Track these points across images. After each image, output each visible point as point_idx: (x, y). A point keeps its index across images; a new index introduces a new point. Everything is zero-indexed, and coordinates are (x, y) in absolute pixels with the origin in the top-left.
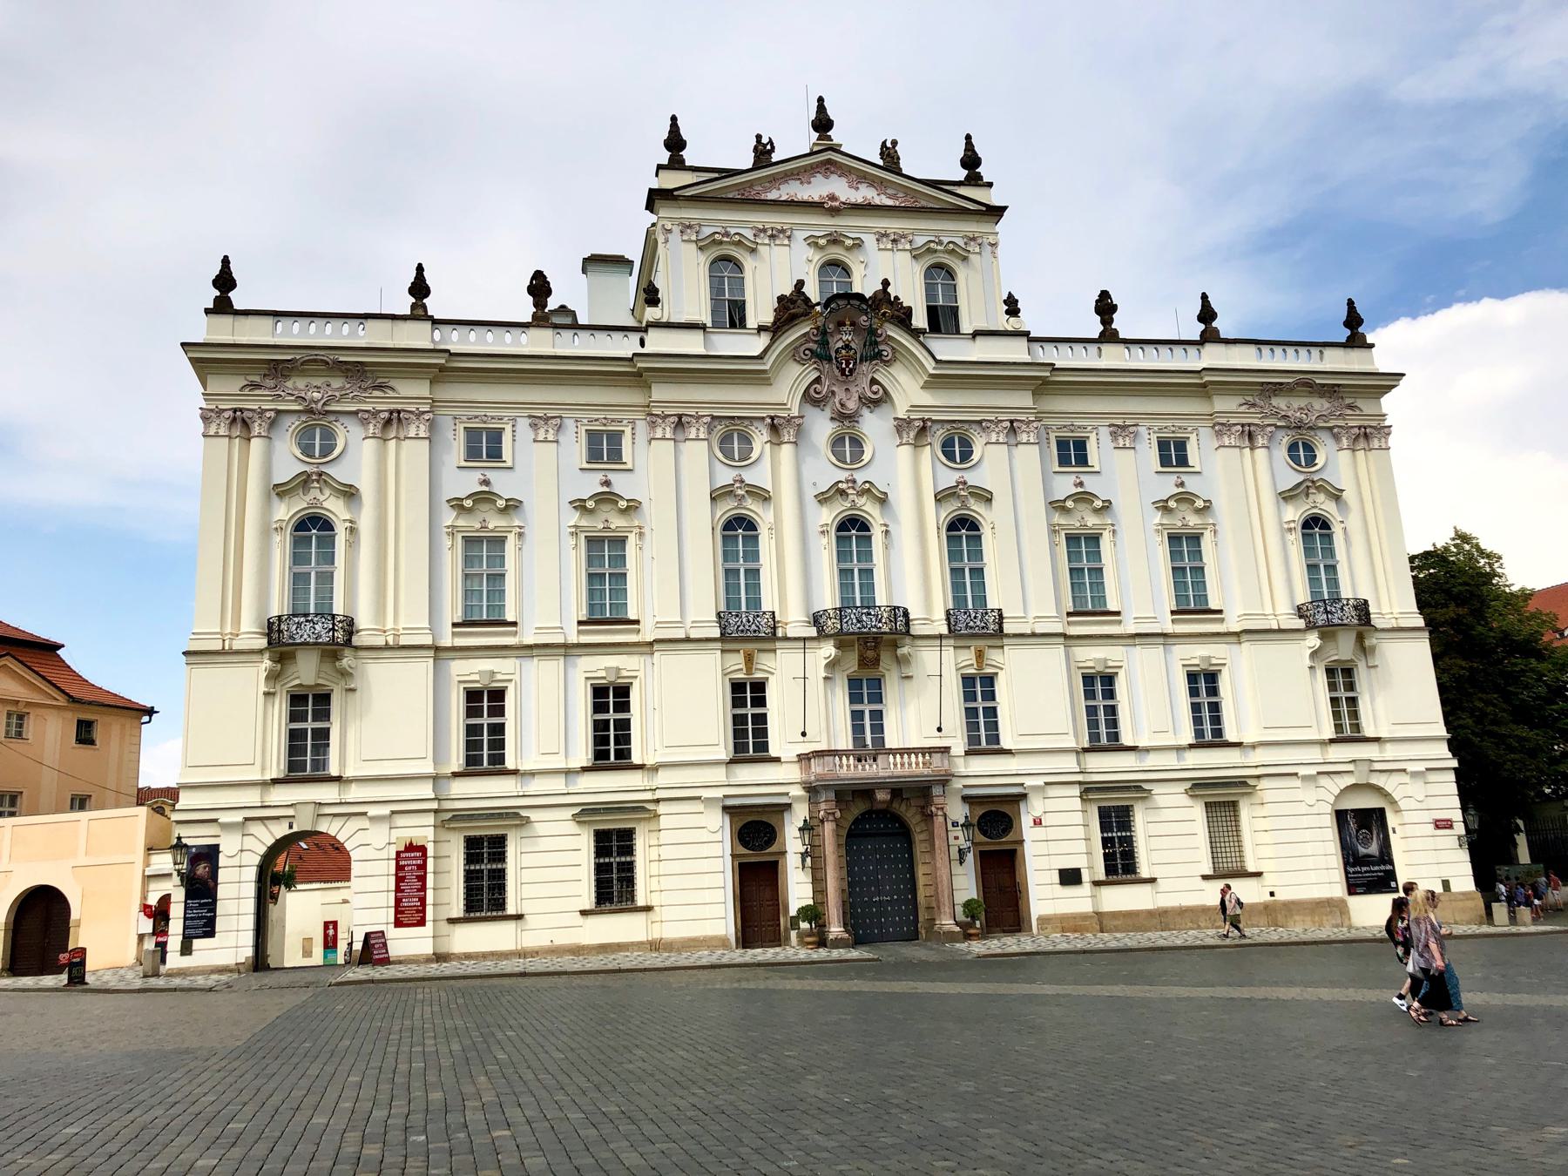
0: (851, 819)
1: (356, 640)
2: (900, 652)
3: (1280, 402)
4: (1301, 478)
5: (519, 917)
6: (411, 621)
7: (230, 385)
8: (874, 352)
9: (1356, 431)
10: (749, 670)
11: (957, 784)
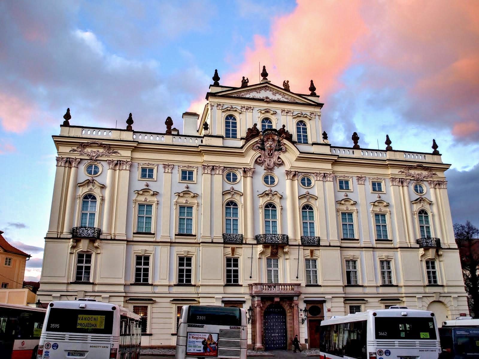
0: (266, 307)
1: (101, 237)
2: (285, 250)
3: (412, 172)
4: (418, 197)
5: (150, 335)
6: (120, 231)
7: (66, 149)
8: (280, 148)
9: (436, 182)
10: (233, 254)
11: (302, 296)
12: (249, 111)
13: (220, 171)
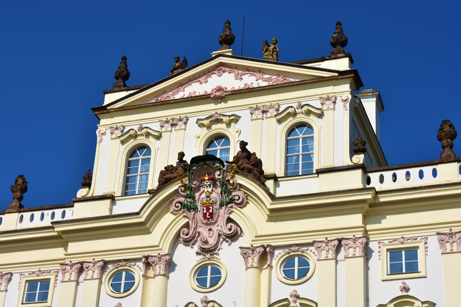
12: (177, 128)
13: (96, 271)
